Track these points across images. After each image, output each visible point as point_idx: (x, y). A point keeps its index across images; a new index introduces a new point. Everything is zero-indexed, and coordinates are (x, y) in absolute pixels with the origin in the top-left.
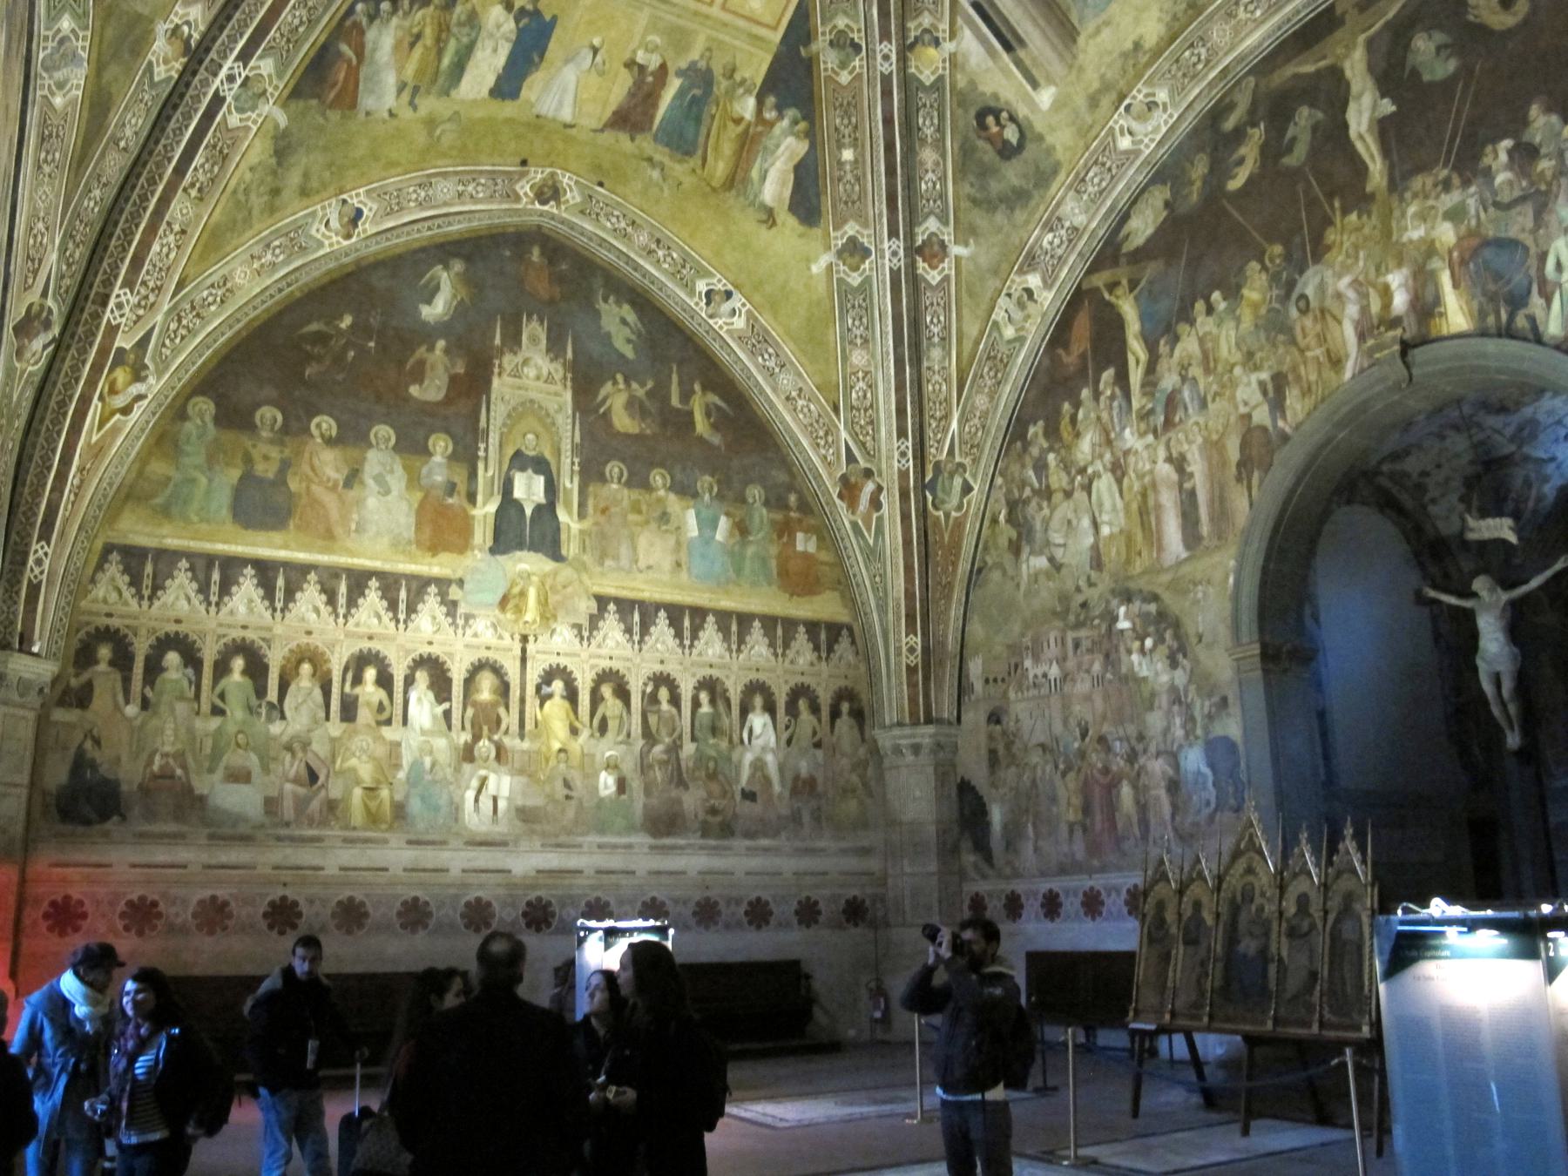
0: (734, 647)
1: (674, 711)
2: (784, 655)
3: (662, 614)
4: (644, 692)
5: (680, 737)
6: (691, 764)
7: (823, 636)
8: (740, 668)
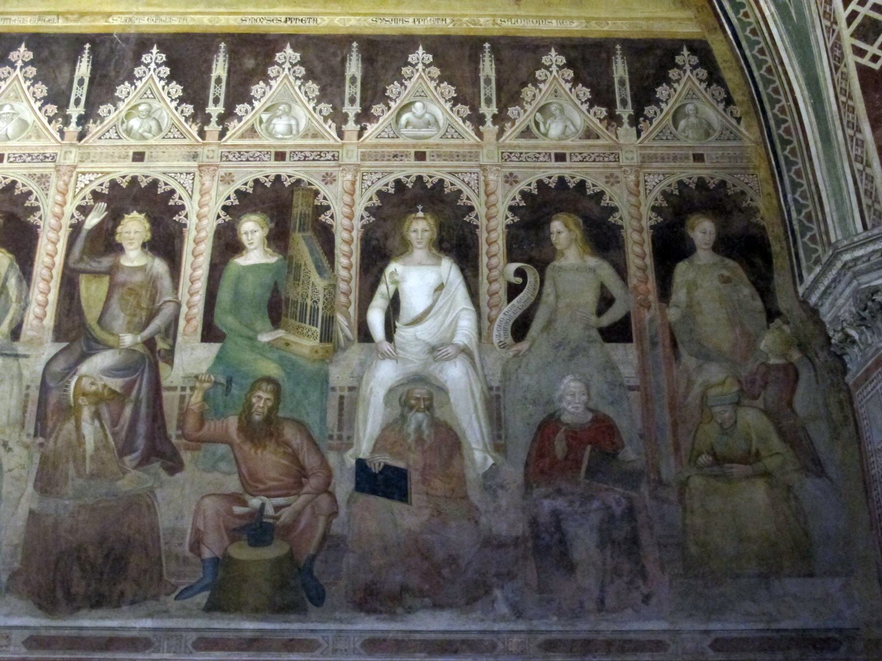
0: (352, 110)
1: (159, 266)
2: (500, 119)
3: (155, 56)
4: (76, 228)
5: (171, 330)
6: (196, 399)
7: (620, 70)
8: (364, 157)
